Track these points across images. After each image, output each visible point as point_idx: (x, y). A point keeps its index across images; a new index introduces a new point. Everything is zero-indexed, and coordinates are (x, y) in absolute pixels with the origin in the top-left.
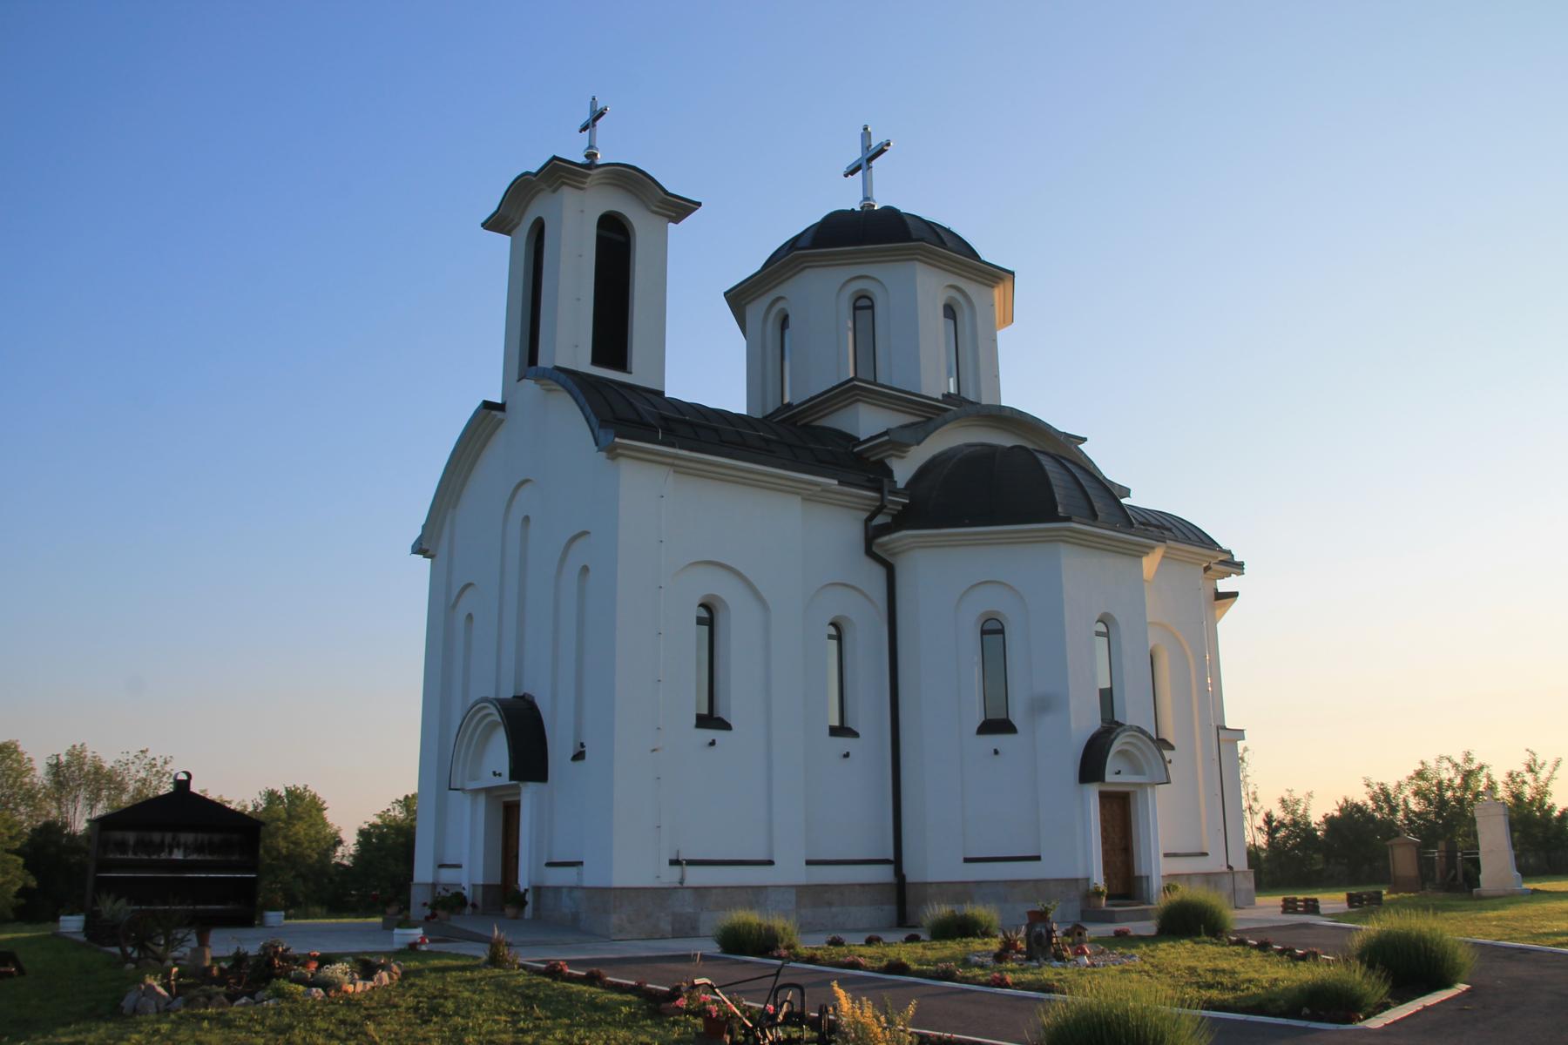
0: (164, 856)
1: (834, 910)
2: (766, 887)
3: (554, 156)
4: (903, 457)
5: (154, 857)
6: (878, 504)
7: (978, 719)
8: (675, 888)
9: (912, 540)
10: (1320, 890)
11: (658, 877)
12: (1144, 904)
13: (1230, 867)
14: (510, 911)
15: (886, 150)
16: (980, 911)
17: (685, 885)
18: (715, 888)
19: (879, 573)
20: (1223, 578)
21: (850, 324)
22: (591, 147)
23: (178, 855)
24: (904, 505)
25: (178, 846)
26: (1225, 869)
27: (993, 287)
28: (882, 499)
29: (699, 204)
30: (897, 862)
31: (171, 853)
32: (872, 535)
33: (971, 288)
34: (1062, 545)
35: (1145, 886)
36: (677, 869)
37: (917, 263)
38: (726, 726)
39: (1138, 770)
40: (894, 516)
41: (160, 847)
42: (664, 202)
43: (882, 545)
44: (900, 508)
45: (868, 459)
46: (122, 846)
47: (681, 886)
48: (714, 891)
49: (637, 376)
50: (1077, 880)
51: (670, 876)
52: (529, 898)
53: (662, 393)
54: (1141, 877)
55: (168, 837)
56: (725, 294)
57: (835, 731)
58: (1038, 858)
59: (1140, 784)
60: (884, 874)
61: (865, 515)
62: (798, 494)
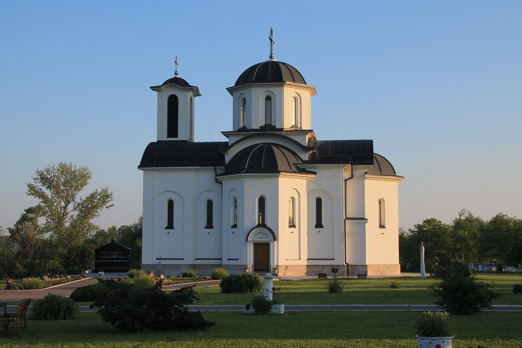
0: (112, 257)
1: (203, 270)
2: (181, 265)
5: (110, 257)
8: (158, 264)
11: (152, 262)
13: (348, 264)
17: (161, 264)
21: (242, 108)
22: (176, 71)
23: (115, 257)
25: (115, 255)
31: (113, 256)
33: (274, 90)
39: (268, 238)
41: (111, 255)
46: (103, 255)
49: (182, 136)
51: (158, 262)
55: (113, 253)
58: (238, 260)
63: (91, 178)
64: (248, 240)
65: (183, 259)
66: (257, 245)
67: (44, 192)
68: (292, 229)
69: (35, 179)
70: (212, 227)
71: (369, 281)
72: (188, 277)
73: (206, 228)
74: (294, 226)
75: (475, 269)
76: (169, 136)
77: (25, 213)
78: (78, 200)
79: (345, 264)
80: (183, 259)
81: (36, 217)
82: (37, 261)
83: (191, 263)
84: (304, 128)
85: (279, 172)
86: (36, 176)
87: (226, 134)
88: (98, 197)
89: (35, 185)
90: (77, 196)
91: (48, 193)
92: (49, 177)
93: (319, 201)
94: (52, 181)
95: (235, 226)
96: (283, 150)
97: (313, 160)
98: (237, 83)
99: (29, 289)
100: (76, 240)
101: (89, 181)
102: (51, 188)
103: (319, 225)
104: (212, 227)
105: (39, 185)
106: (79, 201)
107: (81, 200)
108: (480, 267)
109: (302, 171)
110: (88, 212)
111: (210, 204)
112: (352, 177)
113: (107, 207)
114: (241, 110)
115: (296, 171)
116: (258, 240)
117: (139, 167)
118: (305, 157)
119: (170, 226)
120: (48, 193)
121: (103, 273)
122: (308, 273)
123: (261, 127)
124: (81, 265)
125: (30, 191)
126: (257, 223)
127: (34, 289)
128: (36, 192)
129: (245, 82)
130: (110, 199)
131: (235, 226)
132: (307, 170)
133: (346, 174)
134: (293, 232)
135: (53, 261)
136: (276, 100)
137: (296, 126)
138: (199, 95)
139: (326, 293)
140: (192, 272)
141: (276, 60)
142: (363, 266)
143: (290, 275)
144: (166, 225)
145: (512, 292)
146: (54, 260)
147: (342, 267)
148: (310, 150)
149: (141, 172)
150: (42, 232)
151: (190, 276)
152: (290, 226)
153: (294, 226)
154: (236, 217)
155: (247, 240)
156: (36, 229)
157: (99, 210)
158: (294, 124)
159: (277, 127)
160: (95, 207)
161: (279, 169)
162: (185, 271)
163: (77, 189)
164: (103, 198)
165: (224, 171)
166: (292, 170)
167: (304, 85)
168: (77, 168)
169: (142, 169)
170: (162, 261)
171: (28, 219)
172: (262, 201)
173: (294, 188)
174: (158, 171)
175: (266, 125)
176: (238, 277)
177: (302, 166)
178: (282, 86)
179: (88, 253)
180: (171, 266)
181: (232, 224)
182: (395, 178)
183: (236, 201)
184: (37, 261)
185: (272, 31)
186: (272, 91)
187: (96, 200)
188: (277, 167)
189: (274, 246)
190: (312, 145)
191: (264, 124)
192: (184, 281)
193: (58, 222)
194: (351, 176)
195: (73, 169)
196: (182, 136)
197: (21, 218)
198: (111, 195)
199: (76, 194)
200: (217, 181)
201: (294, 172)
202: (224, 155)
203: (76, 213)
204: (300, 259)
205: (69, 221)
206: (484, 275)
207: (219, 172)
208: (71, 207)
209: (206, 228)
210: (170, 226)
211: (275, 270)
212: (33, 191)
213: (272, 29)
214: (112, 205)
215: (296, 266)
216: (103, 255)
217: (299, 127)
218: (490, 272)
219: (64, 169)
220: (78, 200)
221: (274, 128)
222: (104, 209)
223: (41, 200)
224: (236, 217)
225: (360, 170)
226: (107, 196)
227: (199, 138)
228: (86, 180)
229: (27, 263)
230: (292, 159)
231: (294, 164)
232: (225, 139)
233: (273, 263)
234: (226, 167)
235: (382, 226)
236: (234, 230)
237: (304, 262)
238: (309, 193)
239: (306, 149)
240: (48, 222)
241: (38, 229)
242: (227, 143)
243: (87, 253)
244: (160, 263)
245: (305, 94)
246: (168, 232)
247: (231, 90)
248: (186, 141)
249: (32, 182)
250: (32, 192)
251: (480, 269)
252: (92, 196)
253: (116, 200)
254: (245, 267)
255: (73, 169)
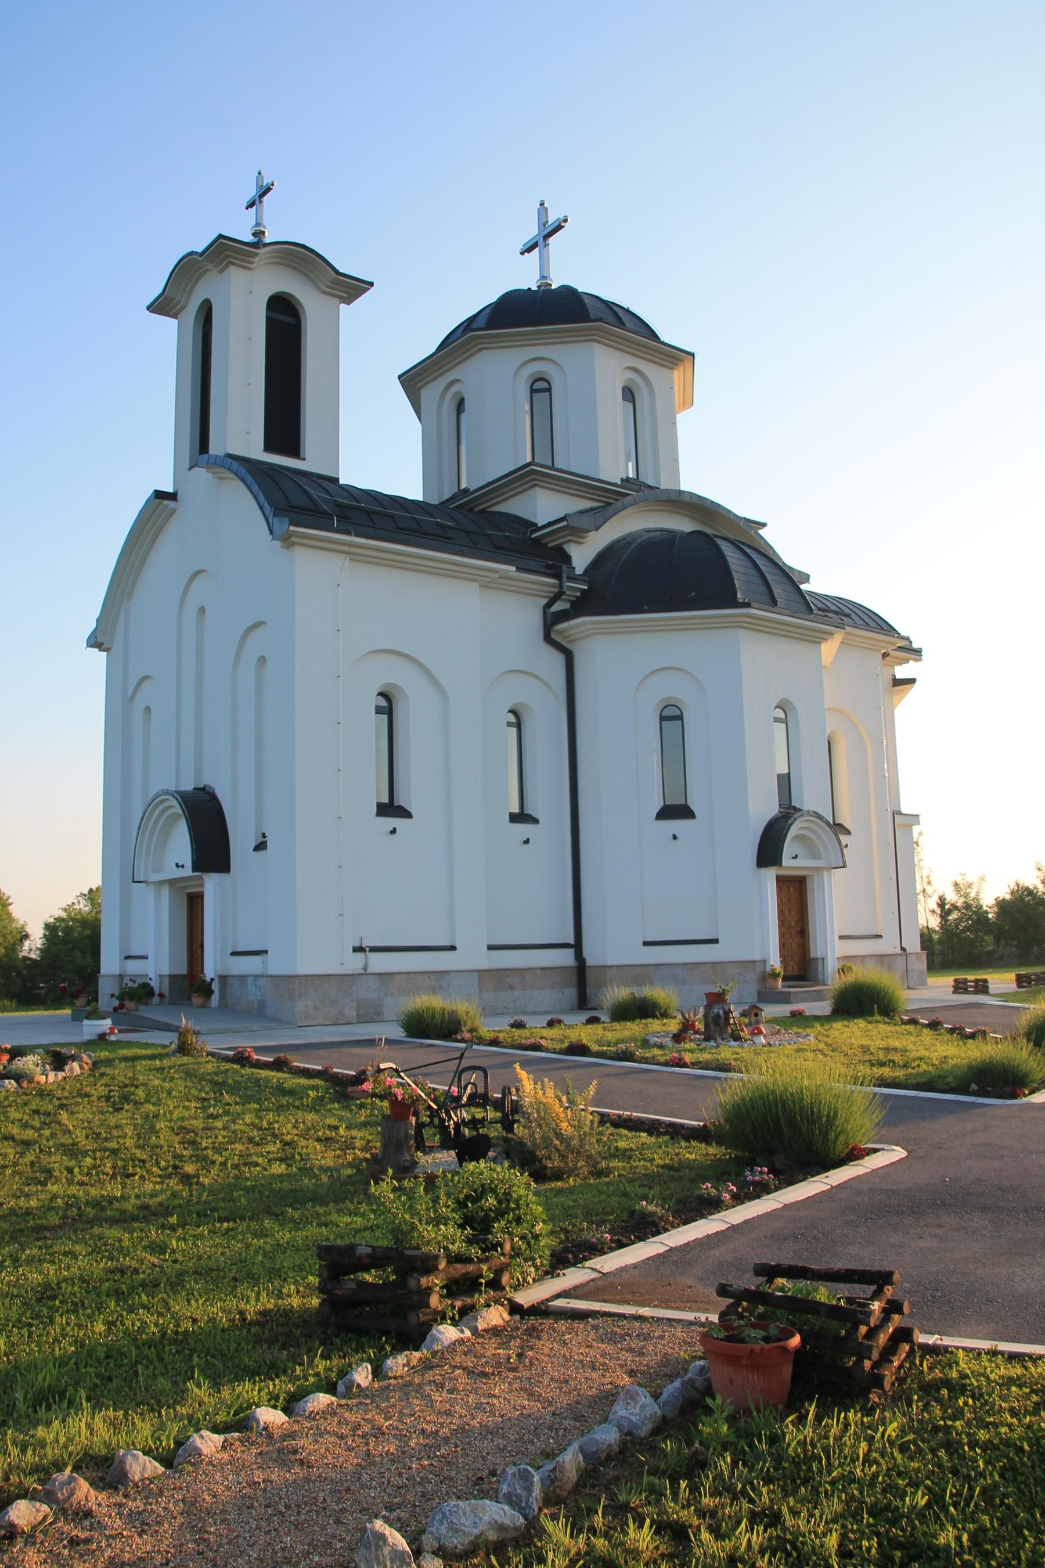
1: (516, 993)
2: (448, 972)
3: (220, 235)
4: (581, 543)
6: (556, 590)
7: (657, 805)
8: (360, 974)
9: (589, 627)
10: (990, 970)
12: (819, 985)
13: (903, 949)
14: (196, 1000)
15: (563, 227)
16: (658, 993)
17: (369, 971)
18: (398, 973)
19: (559, 659)
20: (901, 664)
21: (527, 408)
22: (258, 224)
24: (583, 591)
26: (898, 950)
27: (672, 369)
28: (561, 586)
29: (371, 284)
30: (578, 946)
32: (551, 621)
33: (651, 370)
34: (741, 631)
35: (820, 968)
37: (595, 344)
38: (406, 814)
39: (815, 856)
40: (572, 602)
42: (334, 282)
43: (560, 632)
44: (579, 594)
45: (545, 545)
47: (365, 973)
48: (398, 977)
49: (311, 462)
50: (754, 962)
51: (354, 963)
52: (215, 987)
53: (337, 480)
54: (816, 959)
56: (400, 377)
57: (514, 818)
58: (715, 941)
59: (816, 869)
60: (565, 958)
61: (545, 601)
62: (476, 581)
136: (658, 403)
170: (373, 957)
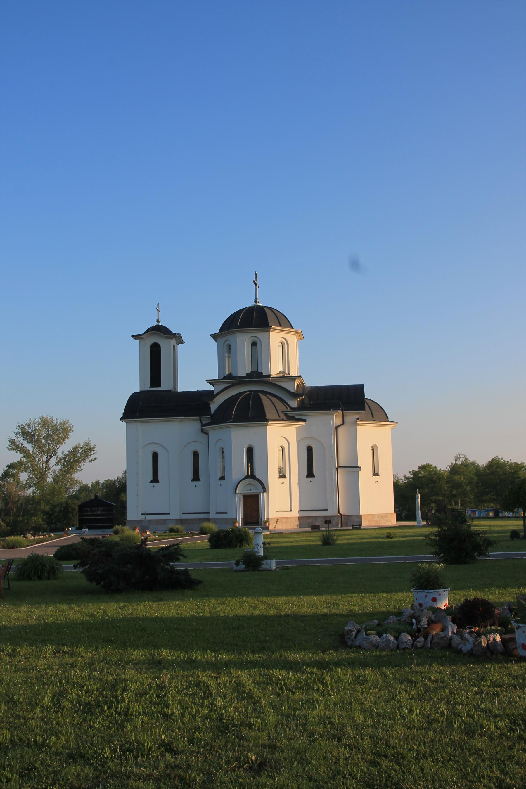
0: (96, 513)
13: (341, 514)
21: (227, 355)
22: (158, 319)
23: (99, 513)
25: (99, 510)
33: (260, 335)
35: (260, 521)
36: (144, 516)
39: (258, 490)
41: (95, 511)
46: (87, 511)
47: (145, 520)
49: (166, 385)
51: (143, 517)
55: (96, 509)
58: (226, 513)
63: (73, 431)
64: (237, 492)
65: (169, 514)
66: (246, 498)
67: (25, 447)
68: (283, 480)
69: (16, 434)
70: (199, 480)
71: (364, 532)
72: (175, 532)
73: (192, 480)
74: (284, 476)
75: (472, 515)
76: (152, 386)
77: (7, 468)
78: (60, 454)
79: (338, 515)
80: (169, 514)
81: (18, 473)
82: (20, 518)
83: (178, 517)
84: (292, 374)
85: (267, 420)
86: (17, 431)
87: (211, 382)
88: (80, 451)
89: (16, 440)
90: (59, 450)
91: (30, 447)
92: (30, 431)
93: (310, 450)
94: (34, 435)
95: (222, 478)
96: (271, 398)
97: (302, 407)
98: (221, 330)
99: (13, 548)
100: (59, 495)
101: (71, 434)
102: (32, 443)
103: (310, 474)
104: (199, 480)
105: (20, 440)
106: (61, 456)
107: (63, 454)
108: (477, 512)
109: (291, 418)
110: (70, 467)
111: (196, 455)
112: (343, 424)
113: (89, 461)
114: (227, 357)
115: (285, 418)
116: (247, 492)
117: (122, 419)
118: (294, 404)
119: (155, 479)
120: (30, 447)
121: (87, 530)
122: (300, 526)
123: (247, 374)
124: (65, 522)
125: (12, 446)
126: (245, 475)
127: (17, 547)
128: (18, 446)
129: (229, 328)
130: (92, 453)
131: (222, 478)
132: (296, 417)
133: (337, 421)
134: (283, 483)
135: (36, 518)
137: (284, 372)
138: (182, 342)
139: (319, 545)
140: (179, 527)
141: (261, 305)
142: (357, 516)
143: (281, 528)
144: (151, 479)
145: (509, 538)
146: (36, 517)
147: (335, 517)
148: (299, 397)
149: (124, 424)
150: (24, 488)
151: (177, 531)
152: (280, 477)
153: (284, 476)
154: (223, 468)
155: (236, 492)
156: (18, 485)
157: (82, 464)
158: (281, 370)
159: (264, 374)
160: (78, 461)
161: (267, 417)
162: (171, 526)
163: (59, 443)
164: (85, 452)
165: (210, 421)
166: (281, 418)
167: (291, 329)
168: (59, 421)
169: (125, 421)
170: (147, 516)
171: (10, 475)
172: (250, 451)
173: (284, 437)
174: (141, 422)
175: (252, 372)
176: (227, 532)
177: (290, 414)
178: (268, 331)
179: (72, 509)
180: (158, 522)
181: (219, 476)
182: (388, 423)
183: (223, 452)
184: (20, 518)
185: (256, 275)
186: (258, 336)
187: (78, 454)
188: (266, 416)
189: (264, 497)
190: (300, 392)
191: (250, 371)
192: (170, 537)
193: (40, 477)
194: (342, 423)
195: (54, 422)
196: (166, 385)
197: (2, 474)
198: (94, 448)
199: (58, 448)
200: (202, 431)
201: (283, 420)
202: (209, 405)
203: (59, 467)
204: (291, 511)
205: (52, 476)
206: (481, 521)
207: (204, 422)
208: (53, 461)
209: (192, 480)
210: (155, 479)
211: (265, 522)
212: (14, 446)
213: (256, 273)
214: (95, 459)
215: (287, 518)
216: (87, 511)
217: (287, 373)
218: (488, 518)
219: (45, 422)
220: (60, 454)
221: (260, 375)
222: (87, 463)
223: (22, 455)
224: (223, 468)
225: (351, 416)
226: (90, 450)
227: (183, 386)
228: (67, 434)
229: (10, 520)
230: (281, 407)
231: (282, 412)
232: (210, 388)
233: (264, 516)
234: (212, 416)
235: (376, 474)
236: (222, 482)
237: (296, 513)
238: (299, 442)
239: (294, 396)
240: (30, 478)
241: (20, 485)
242: (212, 392)
243: (70, 510)
244: (145, 518)
245: (292, 339)
246: (153, 486)
247: (215, 337)
248: (170, 391)
249: (14, 437)
250: (13, 447)
251: (477, 514)
252: (75, 450)
253: (99, 453)
254: (234, 521)
255: (54, 422)
